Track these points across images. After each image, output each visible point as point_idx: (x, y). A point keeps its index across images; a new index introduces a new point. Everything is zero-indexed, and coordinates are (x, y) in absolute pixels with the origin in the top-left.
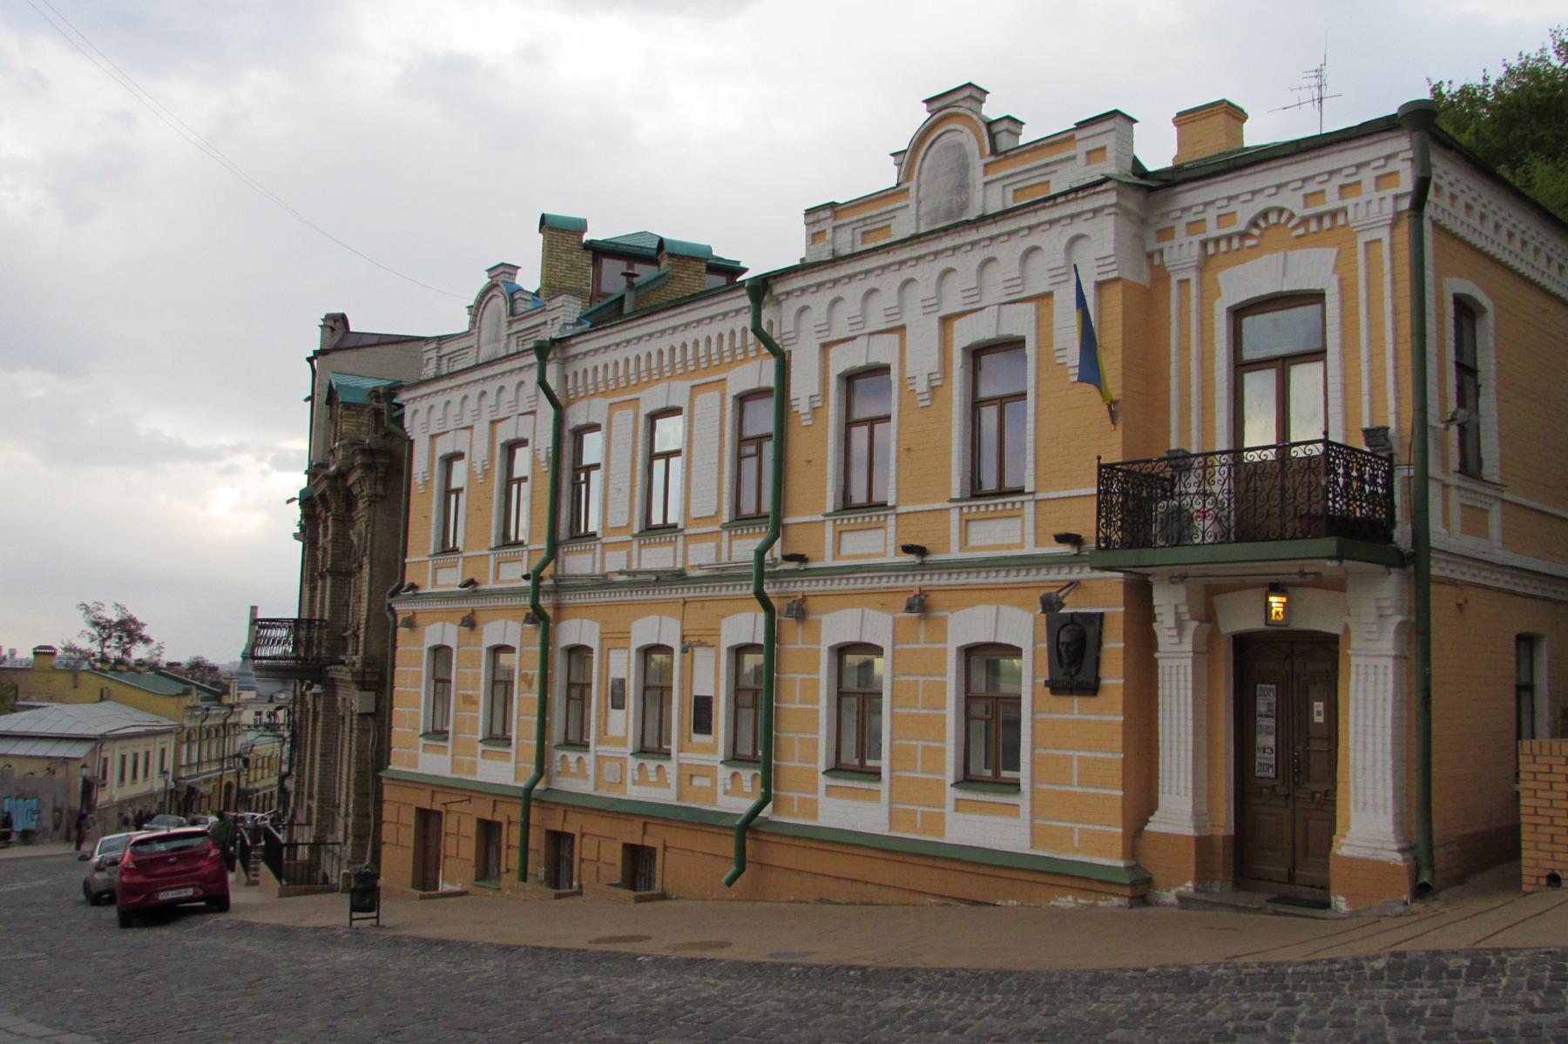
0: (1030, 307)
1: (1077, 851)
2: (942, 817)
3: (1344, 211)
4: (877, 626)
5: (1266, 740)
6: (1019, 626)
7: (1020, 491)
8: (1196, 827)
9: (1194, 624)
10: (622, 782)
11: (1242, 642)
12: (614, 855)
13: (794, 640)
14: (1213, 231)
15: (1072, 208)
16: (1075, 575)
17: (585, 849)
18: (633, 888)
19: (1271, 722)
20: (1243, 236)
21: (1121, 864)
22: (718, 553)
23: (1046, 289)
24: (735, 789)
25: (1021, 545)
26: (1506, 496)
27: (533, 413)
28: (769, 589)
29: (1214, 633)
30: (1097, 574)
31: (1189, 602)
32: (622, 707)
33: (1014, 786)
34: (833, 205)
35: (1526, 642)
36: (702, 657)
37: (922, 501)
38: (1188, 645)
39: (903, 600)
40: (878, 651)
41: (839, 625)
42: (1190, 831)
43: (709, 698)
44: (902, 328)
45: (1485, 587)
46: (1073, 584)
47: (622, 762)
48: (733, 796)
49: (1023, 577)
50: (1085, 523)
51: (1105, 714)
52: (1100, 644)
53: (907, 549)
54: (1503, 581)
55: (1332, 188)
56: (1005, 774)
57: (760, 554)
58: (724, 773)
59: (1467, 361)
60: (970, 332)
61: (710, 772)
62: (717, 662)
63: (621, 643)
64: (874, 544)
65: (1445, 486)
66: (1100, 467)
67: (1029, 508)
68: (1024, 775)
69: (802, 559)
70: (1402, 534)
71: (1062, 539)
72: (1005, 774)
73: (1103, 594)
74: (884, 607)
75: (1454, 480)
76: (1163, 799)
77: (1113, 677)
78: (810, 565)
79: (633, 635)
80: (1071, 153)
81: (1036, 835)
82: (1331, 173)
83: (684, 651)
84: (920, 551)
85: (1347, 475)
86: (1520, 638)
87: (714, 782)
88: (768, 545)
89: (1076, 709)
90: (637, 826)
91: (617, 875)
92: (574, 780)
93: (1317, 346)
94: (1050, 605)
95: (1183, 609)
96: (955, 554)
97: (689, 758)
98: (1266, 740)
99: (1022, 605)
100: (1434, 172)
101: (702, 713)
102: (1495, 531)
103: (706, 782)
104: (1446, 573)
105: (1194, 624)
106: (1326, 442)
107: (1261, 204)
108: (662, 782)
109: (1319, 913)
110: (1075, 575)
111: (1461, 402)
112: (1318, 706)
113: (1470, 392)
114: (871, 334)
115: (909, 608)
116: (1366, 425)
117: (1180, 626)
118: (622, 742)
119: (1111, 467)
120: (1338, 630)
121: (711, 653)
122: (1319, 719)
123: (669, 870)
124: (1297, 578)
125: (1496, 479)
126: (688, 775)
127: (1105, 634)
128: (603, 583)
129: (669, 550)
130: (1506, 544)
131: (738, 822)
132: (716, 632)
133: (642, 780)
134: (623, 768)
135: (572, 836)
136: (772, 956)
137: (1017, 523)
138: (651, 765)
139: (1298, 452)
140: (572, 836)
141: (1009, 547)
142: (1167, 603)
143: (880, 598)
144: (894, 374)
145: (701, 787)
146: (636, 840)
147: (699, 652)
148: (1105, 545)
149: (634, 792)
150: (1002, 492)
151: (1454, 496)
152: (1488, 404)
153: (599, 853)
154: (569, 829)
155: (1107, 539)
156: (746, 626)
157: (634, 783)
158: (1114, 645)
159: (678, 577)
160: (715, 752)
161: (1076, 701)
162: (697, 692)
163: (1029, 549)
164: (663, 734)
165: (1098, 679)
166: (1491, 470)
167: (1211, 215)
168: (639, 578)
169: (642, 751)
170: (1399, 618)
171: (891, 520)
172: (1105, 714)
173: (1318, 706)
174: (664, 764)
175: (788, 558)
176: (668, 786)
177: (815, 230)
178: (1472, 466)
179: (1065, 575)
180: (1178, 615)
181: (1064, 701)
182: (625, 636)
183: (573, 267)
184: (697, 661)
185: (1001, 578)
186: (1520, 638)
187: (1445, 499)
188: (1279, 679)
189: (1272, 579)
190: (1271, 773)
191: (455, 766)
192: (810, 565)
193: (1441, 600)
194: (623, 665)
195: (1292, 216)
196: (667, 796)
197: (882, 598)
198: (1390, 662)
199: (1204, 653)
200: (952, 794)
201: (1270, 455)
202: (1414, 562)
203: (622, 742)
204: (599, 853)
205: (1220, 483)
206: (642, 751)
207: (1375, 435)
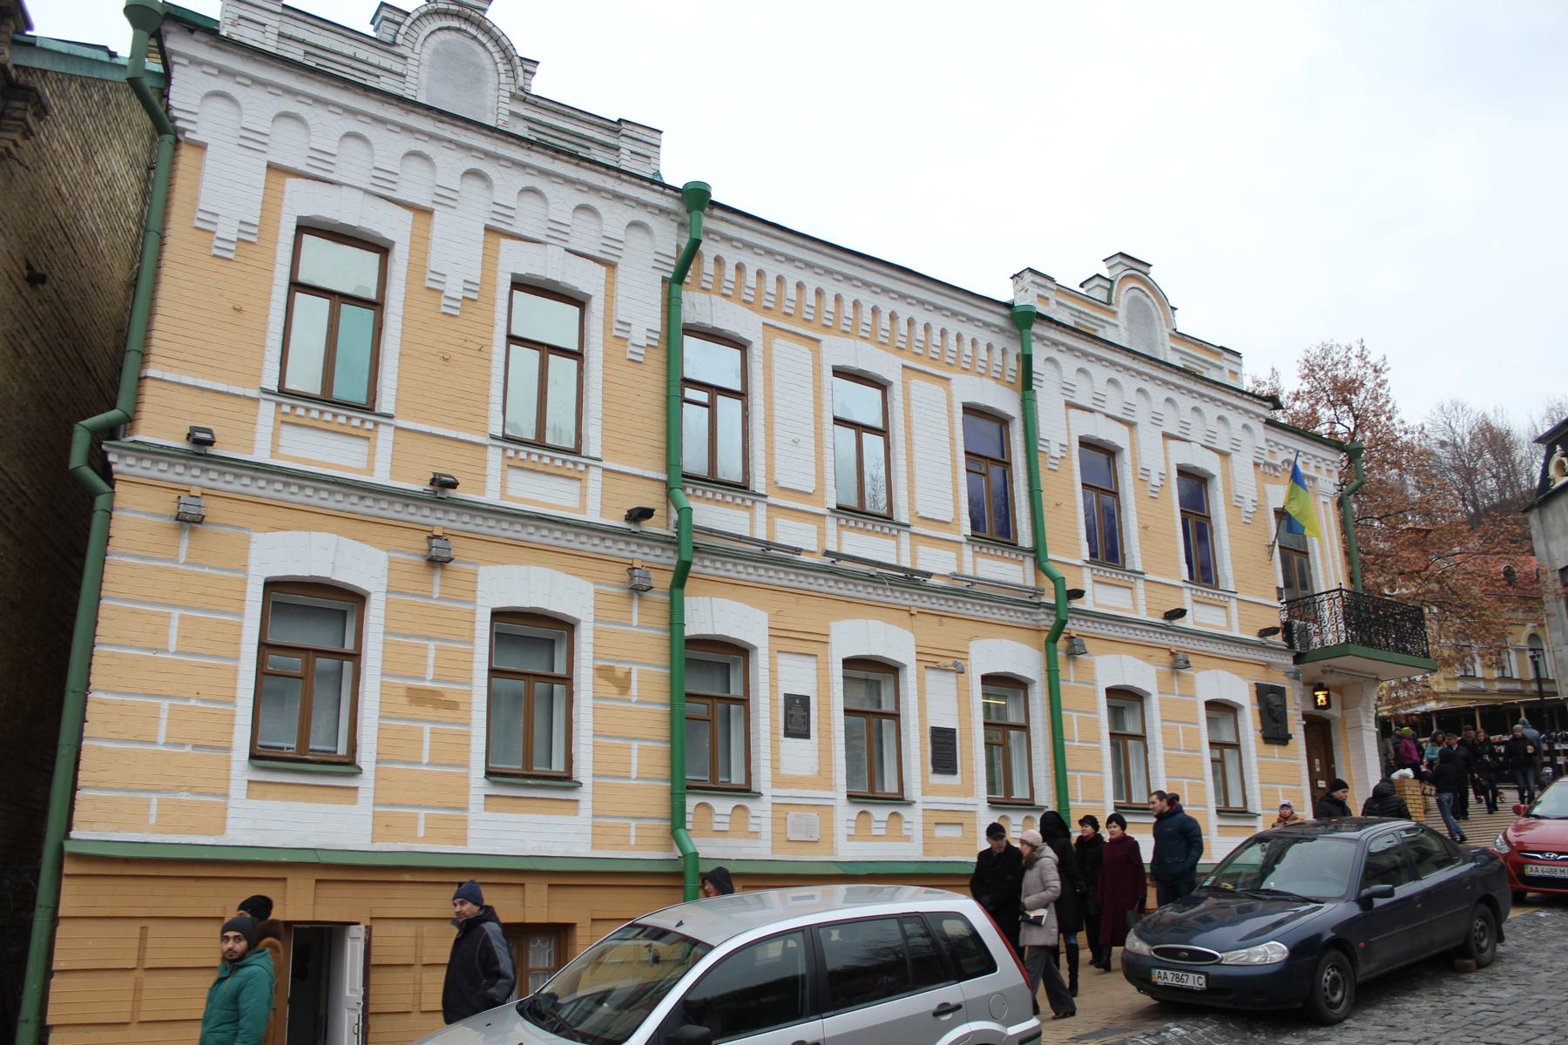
0: (1217, 456)
4: (1138, 672)
6: (1239, 690)
20: (1275, 468)
22: (960, 565)
27: (610, 266)
34: (1052, 279)
37: (1160, 574)
43: (953, 731)
47: (826, 809)
55: (1313, 463)
63: (812, 648)
67: (1233, 603)
74: (1147, 658)
79: (834, 639)
92: (729, 841)
103: (955, 832)
114: (1107, 416)
128: (772, 555)
129: (891, 543)
138: (880, 813)
156: (1017, 655)
159: (911, 579)
168: (843, 564)
174: (901, 810)
176: (907, 838)
177: (1041, 292)
182: (823, 640)
191: (381, 826)
194: (815, 678)
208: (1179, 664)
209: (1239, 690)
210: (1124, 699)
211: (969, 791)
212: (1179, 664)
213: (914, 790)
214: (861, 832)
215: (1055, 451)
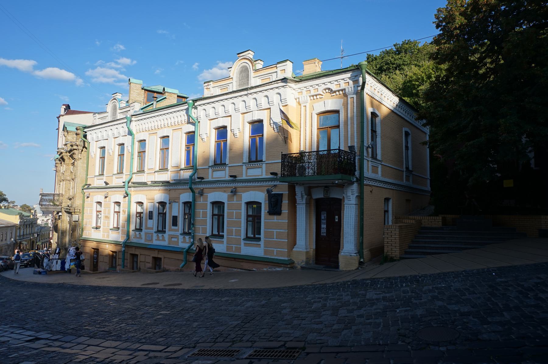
1: (275, 256)
2: (240, 248)
3: (345, 89)
4: (222, 196)
5: (324, 226)
6: (260, 196)
7: (262, 161)
8: (306, 249)
9: (306, 196)
10: (152, 240)
11: (318, 201)
12: (150, 259)
13: (200, 201)
14: (313, 93)
15: (276, 85)
16: (276, 183)
17: (141, 258)
18: (155, 269)
19: (325, 221)
21: (286, 259)
23: (269, 107)
24: (184, 242)
25: (262, 175)
26: (383, 163)
28: (193, 186)
29: (311, 198)
30: (281, 183)
31: (304, 191)
32: (152, 219)
33: (259, 239)
35: (387, 200)
36: (175, 206)
37: (234, 163)
38: (304, 202)
39: (230, 190)
40: (224, 203)
41: (213, 196)
42: (305, 250)
44: (230, 116)
45: (377, 186)
46: (275, 186)
48: (183, 243)
49: (262, 184)
50: (278, 169)
51: (283, 220)
52: (282, 201)
53: (231, 176)
54: (381, 185)
56: (257, 236)
57: (191, 177)
58: (181, 237)
59: (374, 129)
60: (250, 117)
61: (176, 237)
62: (179, 206)
64: (222, 174)
65: (368, 161)
66: (282, 155)
67: (264, 166)
68: (262, 236)
69: (202, 178)
70: (357, 173)
71: (272, 174)
72: (257, 236)
73: (282, 189)
74: (225, 191)
75: (370, 159)
76: (298, 242)
77: (285, 210)
78: (205, 180)
80: (276, 70)
81: (266, 252)
82: (342, 79)
83: (169, 203)
84: (235, 177)
85: (344, 158)
86: (385, 199)
87: (178, 240)
88: (194, 174)
89: (275, 219)
90: (157, 252)
91: (150, 265)
93: (336, 124)
94: (269, 192)
95: (303, 192)
96: (244, 177)
97: (172, 233)
98: (324, 226)
99: (262, 191)
100: (367, 80)
101: (175, 221)
102: (380, 173)
103: (176, 240)
104: (368, 183)
105: (306, 196)
106: (339, 149)
107: (324, 87)
108: (163, 240)
109: (336, 270)
110: (276, 183)
111: (372, 140)
112: (337, 217)
113: (375, 137)
115: (232, 192)
116: (349, 145)
117: (302, 197)
118: (152, 229)
119: (285, 155)
120: (342, 198)
121: (177, 204)
122: (337, 220)
123: (165, 264)
124: (331, 185)
125: (380, 159)
126: (171, 237)
127: (283, 199)
130: (382, 175)
131: (184, 250)
132: (179, 198)
133: (158, 239)
134: (152, 236)
135: (137, 255)
136: (194, 287)
137: (260, 170)
138: (160, 235)
139: (332, 152)
140: (137, 255)
141: (258, 176)
142: (299, 190)
143: (223, 189)
144: (229, 129)
145: (174, 241)
146: (156, 255)
147: (173, 204)
148: (283, 175)
149: (155, 242)
150: (257, 161)
151: (370, 163)
152: (379, 140)
153: (145, 260)
154: (136, 253)
155: (284, 174)
156: (186, 197)
157: (156, 240)
158: (285, 202)
160: (178, 231)
161: (275, 217)
162: (173, 215)
163: (264, 176)
164: (164, 226)
165: (281, 211)
166: (379, 157)
167: (311, 88)
169: (158, 231)
170: (357, 195)
171: (227, 168)
172: (283, 220)
173: (337, 217)
175: (198, 178)
178: (375, 156)
179: (273, 183)
180: (302, 194)
181: (272, 217)
183: (139, 94)
184: (173, 206)
185: (256, 184)
186: (385, 199)
187: (368, 164)
188: (327, 211)
189: (325, 185)
190: (325, 235)
192: (205, 180)
193: (366, 190)
195: (332, 90)
196: (166, 243)
197: (225, 189)
198: (354, 206)
199: (308, 204)
200: (243, 242)
201: (325, 153)
202: (360, 181)
203: (152, 229)
204: (145, 260)
205: (313, 160)
206: (158, 231)
207: (351, 148)
208: (234, 192)
209: (260, 196)
210: (218, 205)
211: (178, 230)
212: (234, 192)
213: (167, 230)
214: (158, 239)
215: (204, 136)
